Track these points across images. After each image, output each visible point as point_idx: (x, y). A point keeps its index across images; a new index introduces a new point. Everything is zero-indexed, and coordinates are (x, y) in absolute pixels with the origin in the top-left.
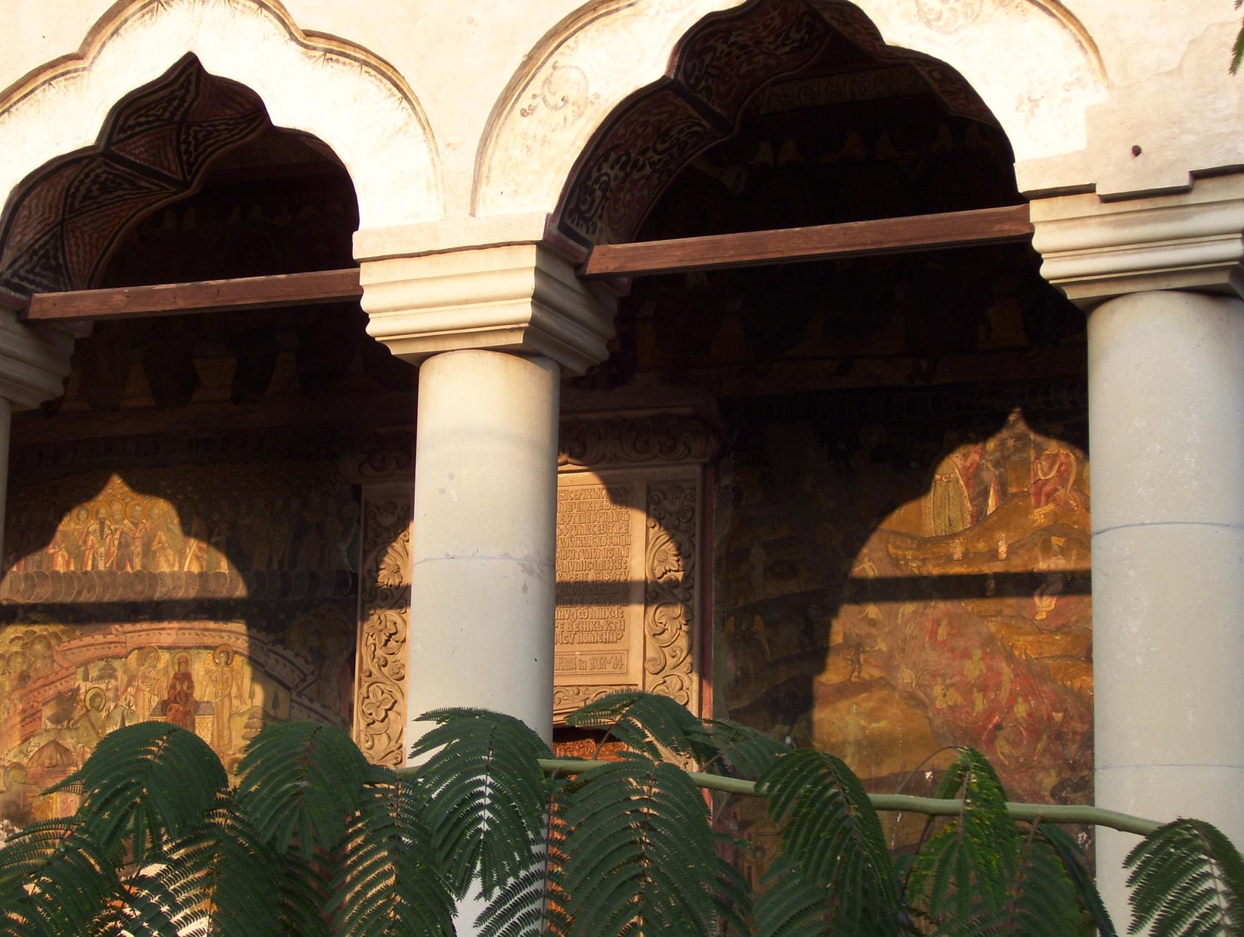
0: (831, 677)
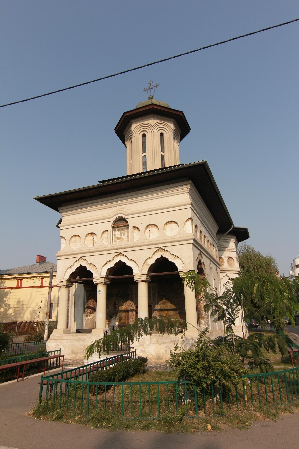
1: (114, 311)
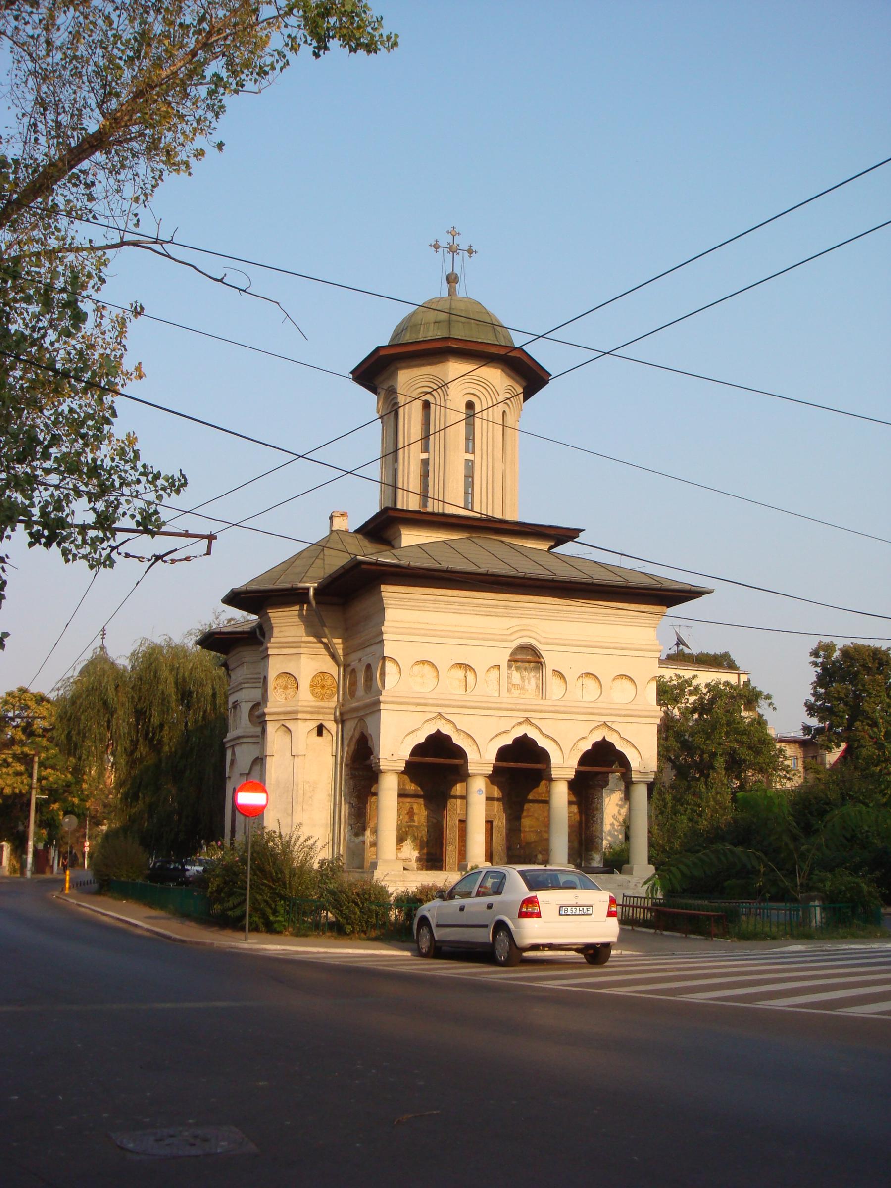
0: (525, 814)
1: (409, 826)
